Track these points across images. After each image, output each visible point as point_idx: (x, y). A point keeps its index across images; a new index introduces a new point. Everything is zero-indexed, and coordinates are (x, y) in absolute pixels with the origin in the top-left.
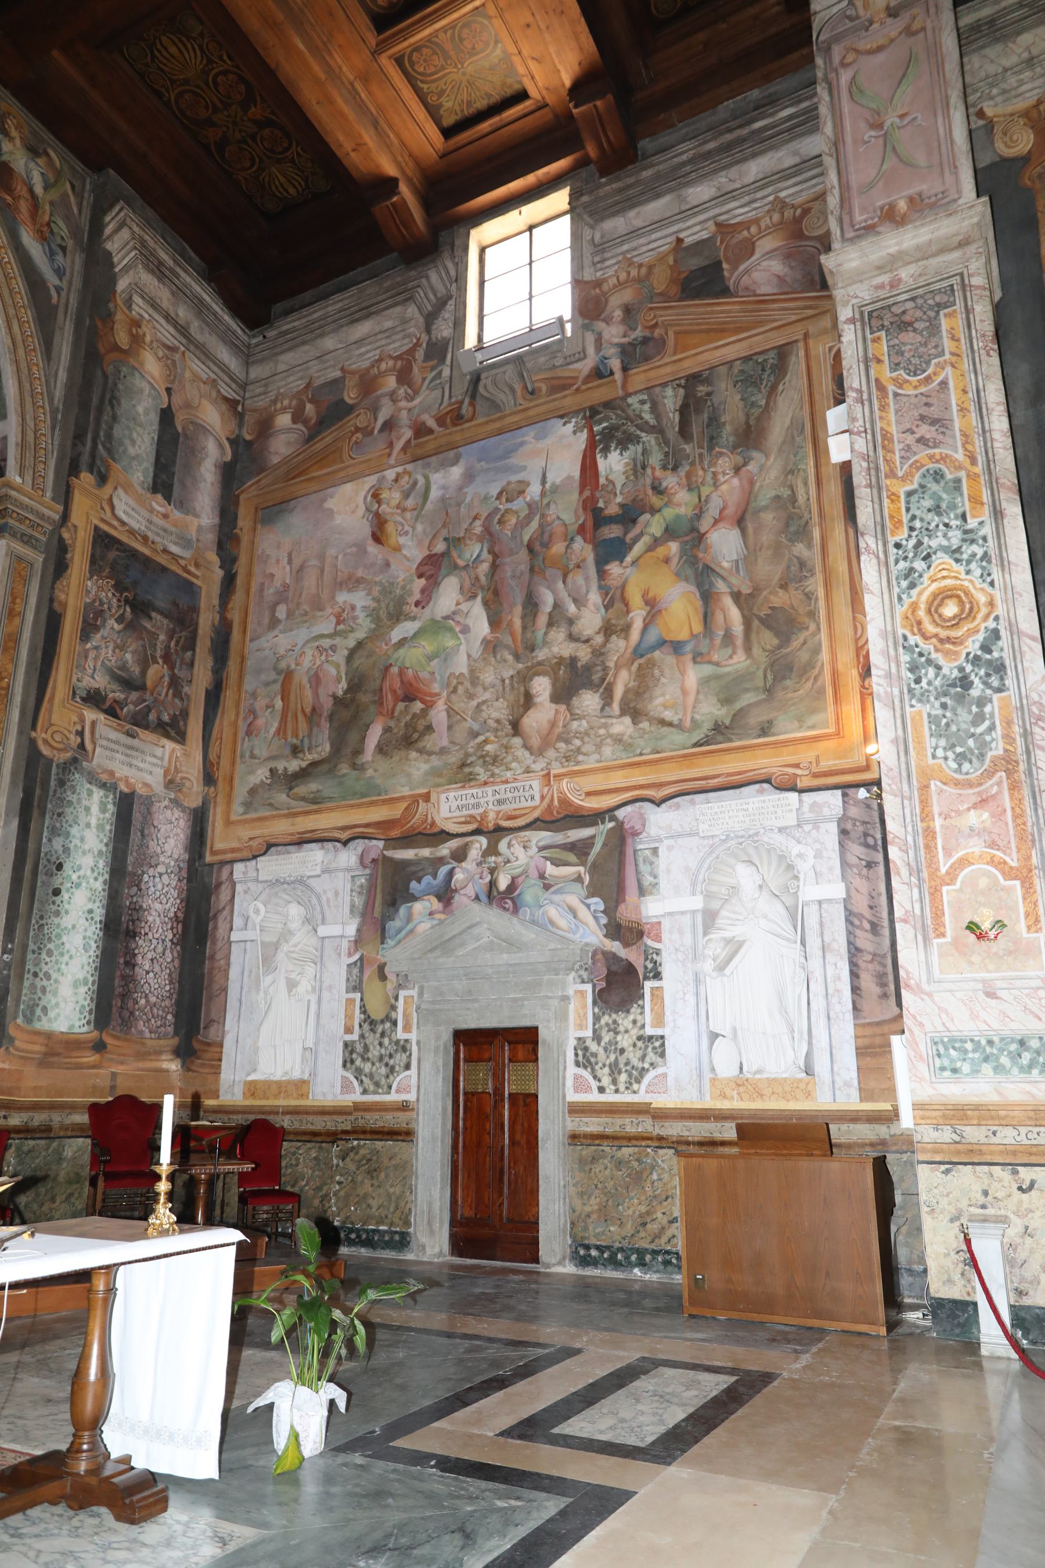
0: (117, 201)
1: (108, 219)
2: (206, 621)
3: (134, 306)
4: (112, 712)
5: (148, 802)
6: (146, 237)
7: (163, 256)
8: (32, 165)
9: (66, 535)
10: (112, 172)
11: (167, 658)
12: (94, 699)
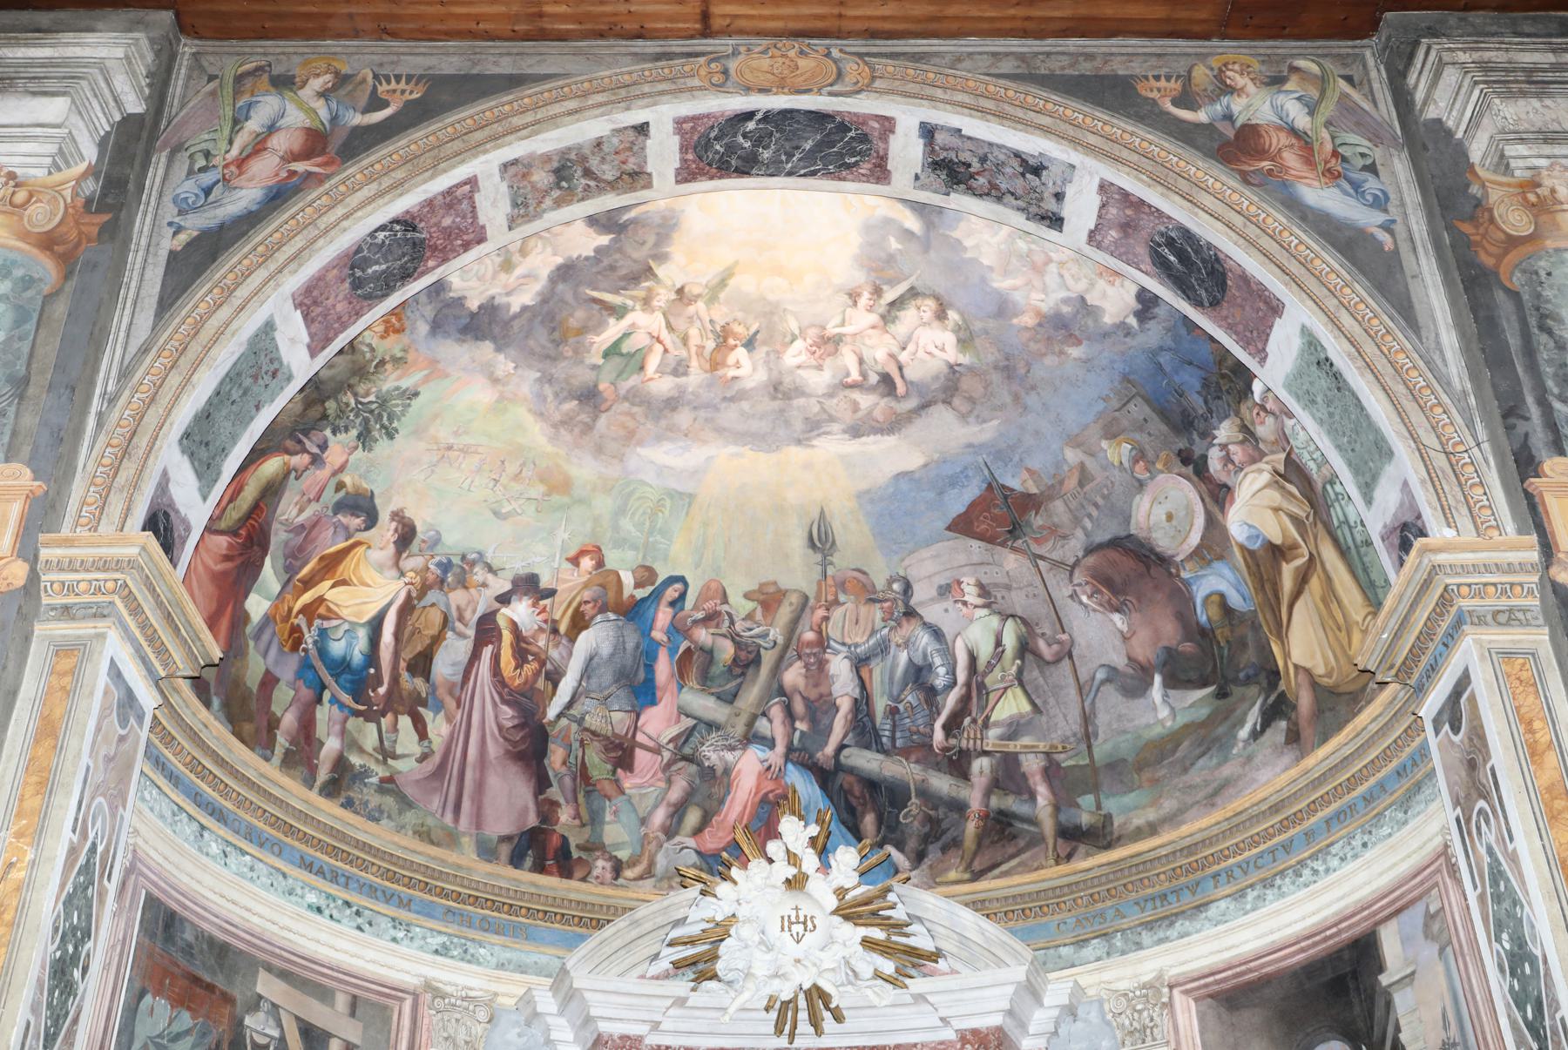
0: (1416, 44)
1: (1411, 79)
3: (1513, 164)
6: (1487, 55)
7: (1527, 58)
8: (1281, 98)
10: (1388, 15)
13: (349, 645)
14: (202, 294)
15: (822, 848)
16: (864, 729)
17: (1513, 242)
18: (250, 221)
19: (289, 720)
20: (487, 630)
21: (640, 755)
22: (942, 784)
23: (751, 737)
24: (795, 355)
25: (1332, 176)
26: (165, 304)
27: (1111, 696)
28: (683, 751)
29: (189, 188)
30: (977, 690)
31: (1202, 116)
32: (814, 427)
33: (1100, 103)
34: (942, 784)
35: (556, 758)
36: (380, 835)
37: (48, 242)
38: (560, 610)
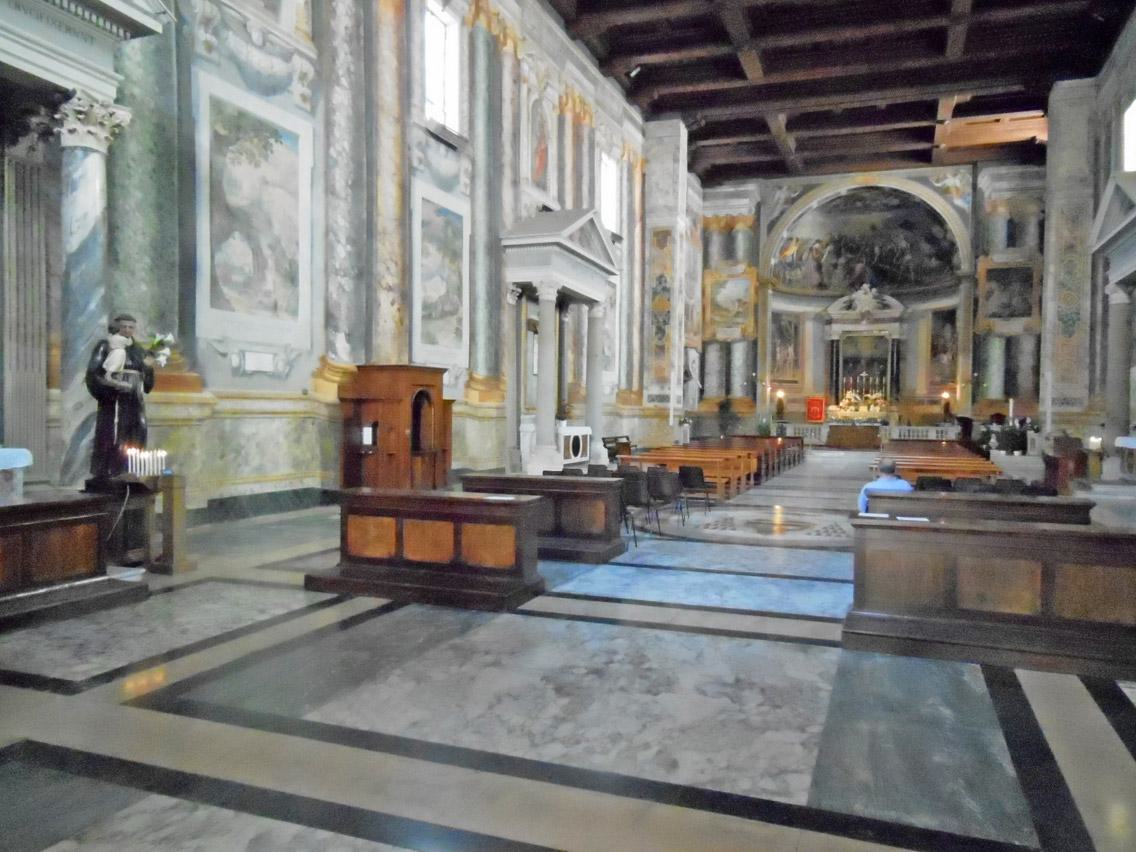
2: (1035, 280)
9: (977, 276)
12: (994, 315)
13: (789, 260)
15: (871, 288)
17: (990, 214)
18: (778, 218)
19: (782, 276)
20: (811, 249)
21: (839, 267)
23: (859, 262)
24: (868, 202)
27: (926, 260)
30: (903, 253)
31: (939, 185)
35: (824, 269)
38: (824, 244)
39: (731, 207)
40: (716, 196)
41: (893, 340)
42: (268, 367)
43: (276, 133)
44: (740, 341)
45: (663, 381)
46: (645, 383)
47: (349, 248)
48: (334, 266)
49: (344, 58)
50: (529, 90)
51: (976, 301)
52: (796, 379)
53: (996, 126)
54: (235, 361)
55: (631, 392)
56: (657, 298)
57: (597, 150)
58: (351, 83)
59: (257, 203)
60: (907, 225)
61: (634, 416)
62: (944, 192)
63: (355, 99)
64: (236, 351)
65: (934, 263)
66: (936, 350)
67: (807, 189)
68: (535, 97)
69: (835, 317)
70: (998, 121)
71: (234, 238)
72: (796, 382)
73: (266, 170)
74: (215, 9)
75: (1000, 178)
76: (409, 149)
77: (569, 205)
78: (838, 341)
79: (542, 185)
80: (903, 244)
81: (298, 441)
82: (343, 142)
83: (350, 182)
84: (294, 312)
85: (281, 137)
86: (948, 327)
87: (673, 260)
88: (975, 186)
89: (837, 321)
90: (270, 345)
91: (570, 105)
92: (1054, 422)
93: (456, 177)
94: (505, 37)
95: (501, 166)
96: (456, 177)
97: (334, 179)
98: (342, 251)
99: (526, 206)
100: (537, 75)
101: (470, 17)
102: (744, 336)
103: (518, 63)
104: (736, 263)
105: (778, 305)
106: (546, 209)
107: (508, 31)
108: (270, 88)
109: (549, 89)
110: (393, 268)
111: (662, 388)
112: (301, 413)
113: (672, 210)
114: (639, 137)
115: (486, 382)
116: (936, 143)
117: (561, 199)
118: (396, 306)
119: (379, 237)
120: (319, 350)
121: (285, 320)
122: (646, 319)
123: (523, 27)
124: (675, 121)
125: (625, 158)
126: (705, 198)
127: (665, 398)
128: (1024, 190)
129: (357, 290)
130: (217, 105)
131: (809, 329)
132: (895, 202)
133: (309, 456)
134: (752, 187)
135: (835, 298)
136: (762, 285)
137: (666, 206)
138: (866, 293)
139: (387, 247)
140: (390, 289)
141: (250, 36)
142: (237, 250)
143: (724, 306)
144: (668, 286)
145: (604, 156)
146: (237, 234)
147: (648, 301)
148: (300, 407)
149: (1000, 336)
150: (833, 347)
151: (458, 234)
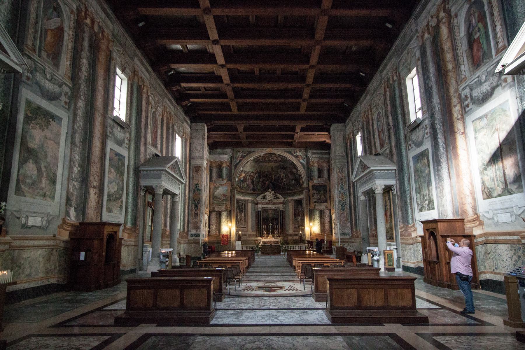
2: (328, 190)
4: (318, 203)
5: (324, 210)
11: (324, 195)
12: (315, 202)
14: (237, 169)
15: (272, 191)
16: (275, 180)
18: (239, 163)
20: (250, 175)
22: (280, 185)
25: (302, 159)
26: (235, 169)
28: (262, 182)
29: (235, 160)
30: (282, 178)
32: (271, 162)
33: (289, 153)
34: (280, 185)
36: (245, 191)
37: (228, 166)
39: (221, 158)
40: (215, 153)
41: (280, 211)
42: (39, 224)
43: (53, 117)
44: (224, 211)
45: (197, 228)
46: (189, 229)
47: (79, 168)
48: (72, 177)
49: (83, 88)
50: (152, 107)
51: (309, 197)
52: (245, 226)
53: (313, 136)
54: (23, 221)
55: (184, 233)
56: (195, 194)
57: (175, 133)
58: (85, 98)
59: (42, 147)
60: (284, 168)
61: (185, 243)
62: (297, 157)
63: (86, 105)
64: (24, 216)
65: (293, 182)
66: (296, 215)
67: (250, 152)
68: (154, 110)
69: (259, 202)
70: (314, 134)
71: (30, 163)
72: (245, 228)
73: (47, 133)
74: (33, 63)
75: (315, 153)
76: (106, 127)
77: (164, 155)
78: (260, 211)
79: (155, 146)
80: (283, 175)
81: (48, 260)
82: (80, 123)
83: (82, 140)
84: (53, 198)
85: (54, 119)
86: (300, 206)
87: (202, 178)
88: (306, 156)
89: (260, 203)
90: (41, 213)
91: (166, 115)
92: (341, 242)
93: (124, 140)
94: (144, 87)
95: (141, 137)
96: (124, 140)
97: (75, 138)
98: (76, 170)
99: (149, 153)
100: (155, 102)
101: (131, 77)
102: (226, 209)
103: (148, 97)
104: (223, 180)
105: (238, 197)
106: (157, 155)
107: (145, 84)
108: (52, 98)
109: (158, 108)
110: (96, 178)
111: (197, 231)
112: (52, 246)
113: (202, 158)
114: (189, 129)
115: (130, 229)
116: (294, 140)
117: (161, 151)
118: (97, 195)
119: (92, 164)
120: (62, 215)
121: (49, 201)
122: (190, 202)
123: (150, 83)
124: (203, 124)
125: (184, 136)
126: (210, 153)
127: (198, 235)
128: (322, 158)
129: (81, 188)
130: (29, 103)
131: (250, 205)
132: (279, 159)
133: (53, 267)
134: (228, 151)
135: (258, 195)
136: (233, 189)
137: (199, 156)
138: (270, 193)
139: (95, 169)
140: (95, 188)
141: (46, 75)
142: (30, 168)
143: (218, 197)
144: (200, 188)
145: (177, 136)
146: (31, 161)
147: (191, 194)
148: (51, 243)
149: (318, 210)
150: (258, 214)
151: (123, 164)
